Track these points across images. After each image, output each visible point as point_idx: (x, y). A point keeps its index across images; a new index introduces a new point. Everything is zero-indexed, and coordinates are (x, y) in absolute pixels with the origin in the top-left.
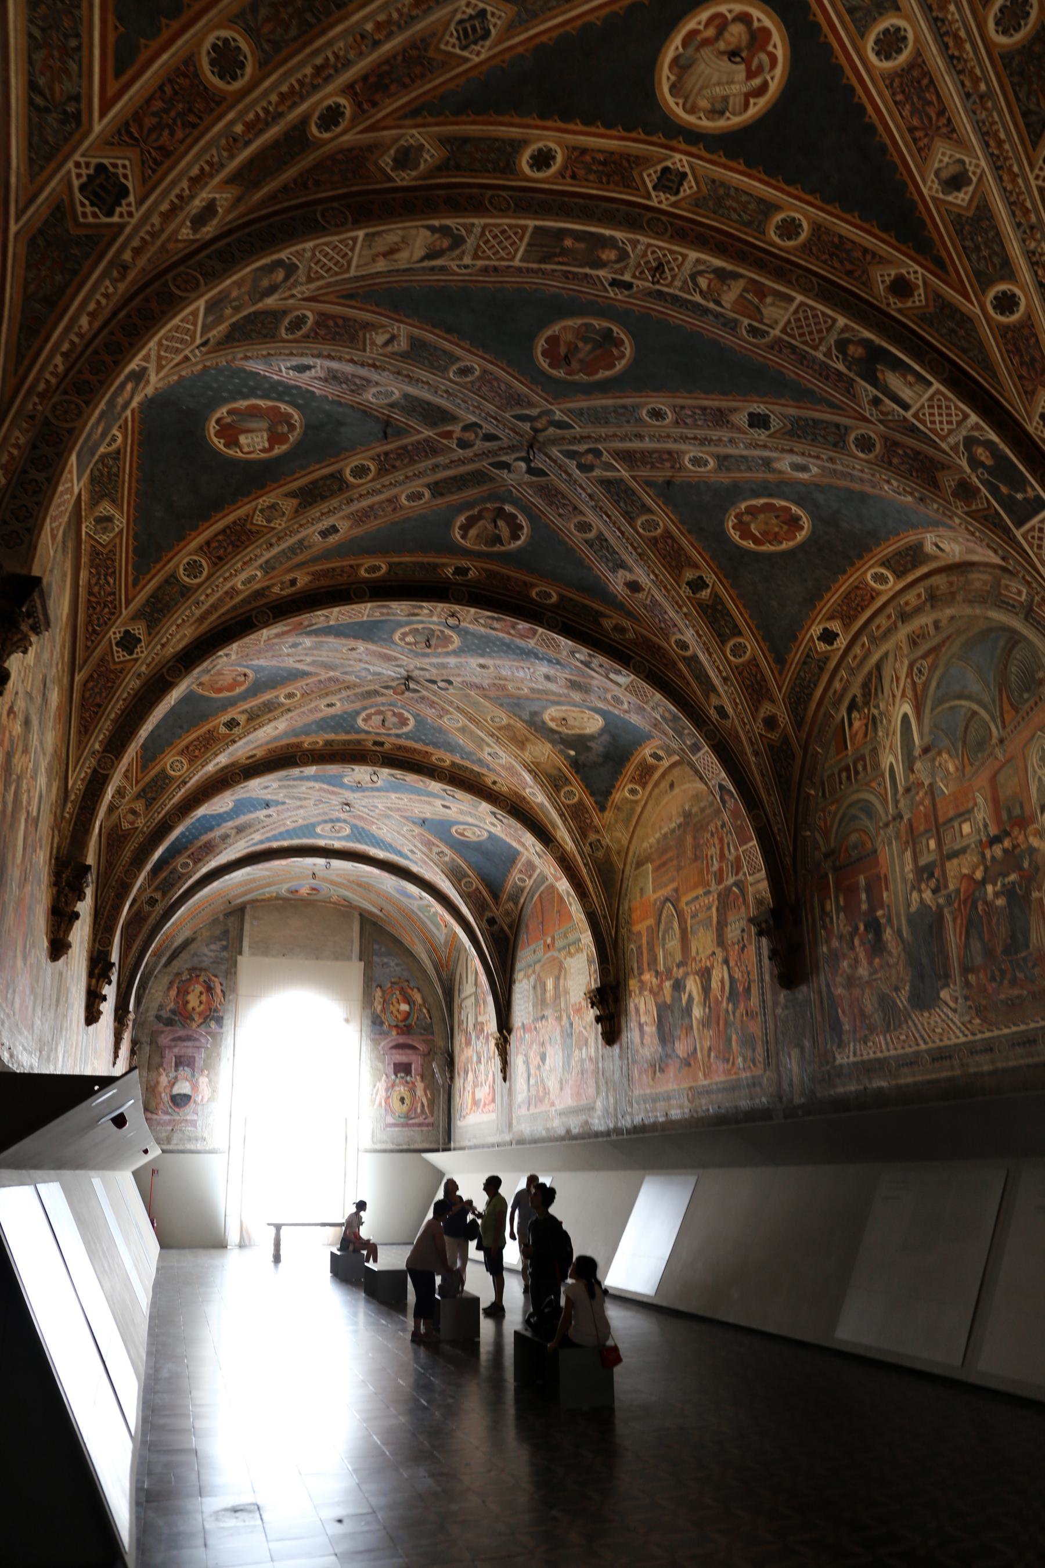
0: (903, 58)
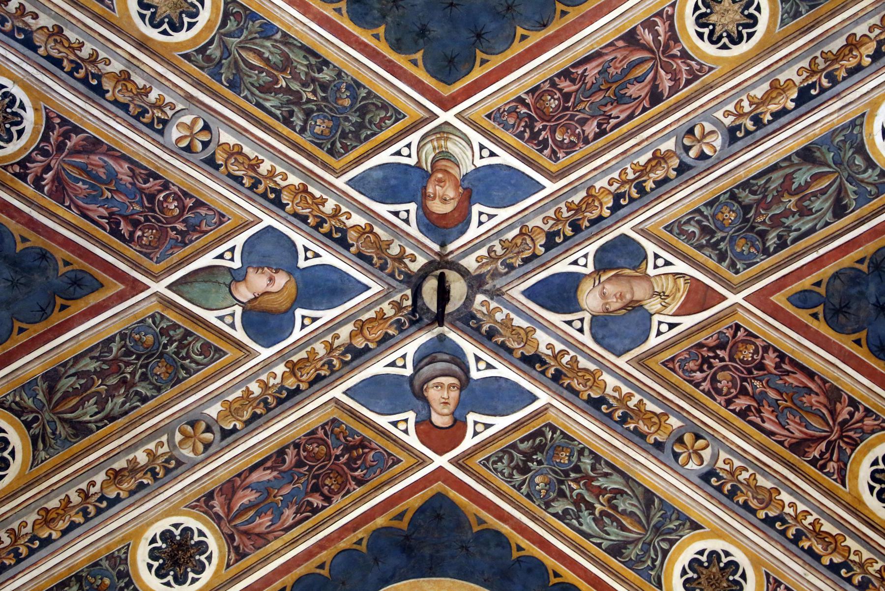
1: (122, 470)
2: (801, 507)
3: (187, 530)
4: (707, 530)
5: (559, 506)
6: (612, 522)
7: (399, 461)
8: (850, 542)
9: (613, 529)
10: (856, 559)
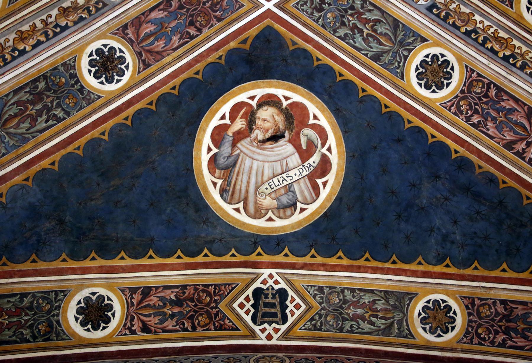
0: (456, 80)
1: (68, 8)
2: (487, 23)
3: (112, 49)
4: (431, 41)
5: (342, 32)
6: (374, 40)
7: (243, 6)
8: (515, 42)
9: (374, 44)
10: (519, 51)
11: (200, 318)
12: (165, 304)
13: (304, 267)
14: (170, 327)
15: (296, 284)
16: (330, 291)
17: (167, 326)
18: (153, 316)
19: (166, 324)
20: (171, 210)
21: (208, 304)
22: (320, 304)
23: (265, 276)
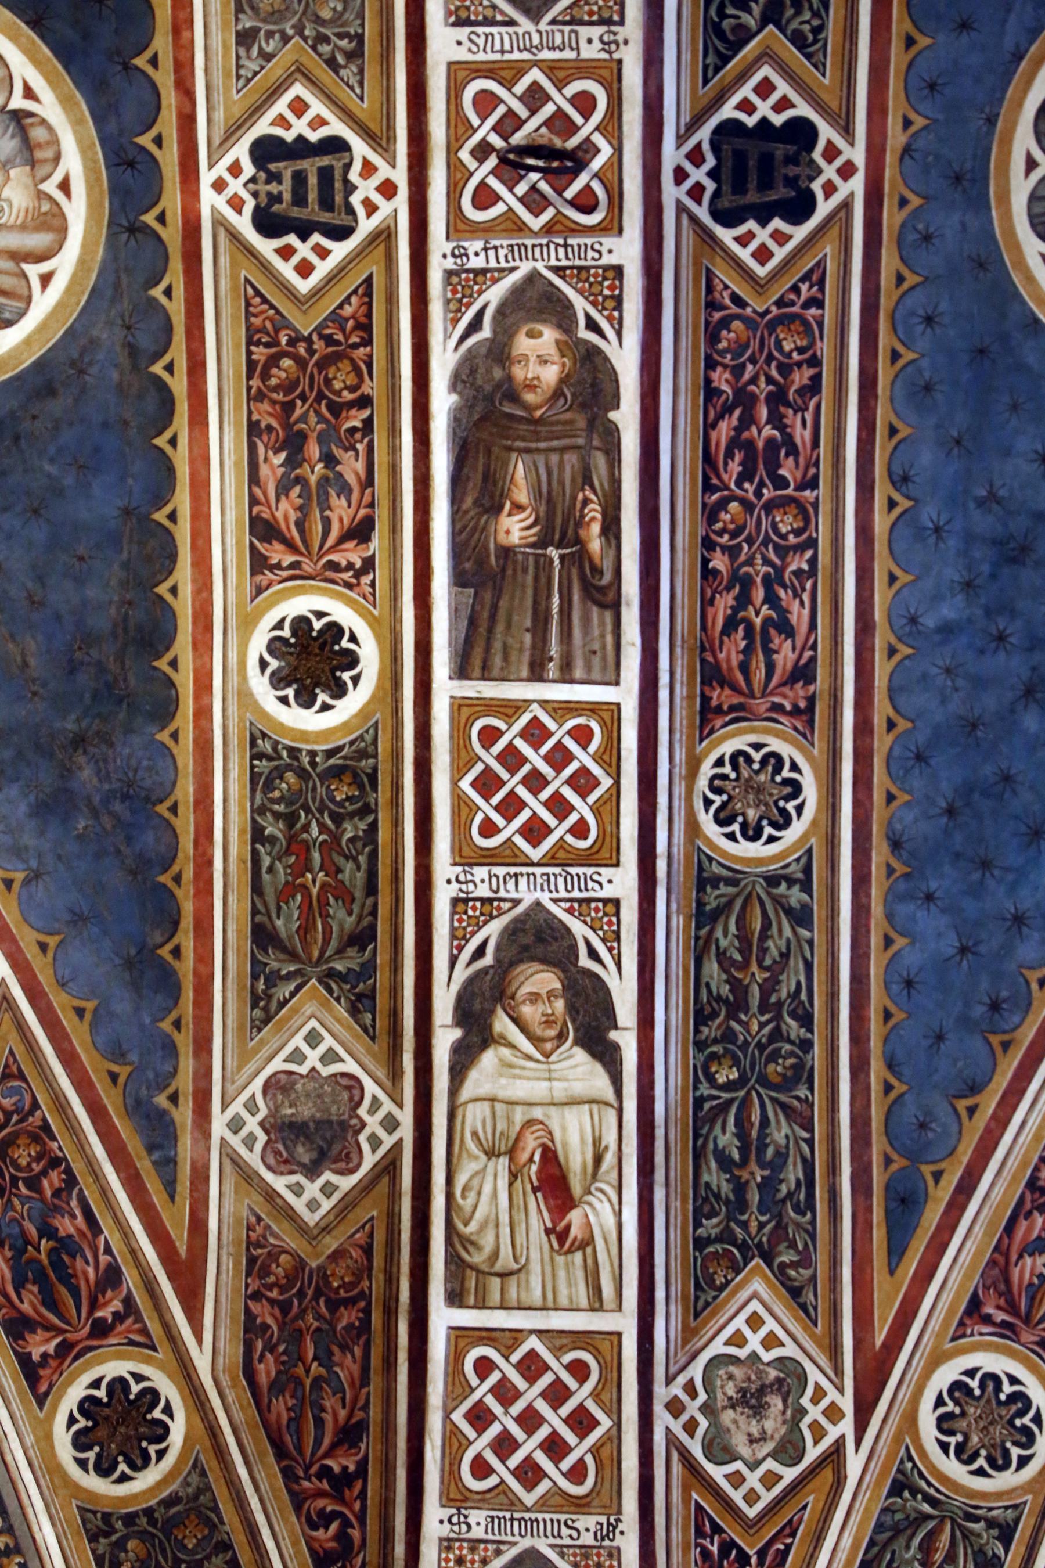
11: (337, 385)
12: (298, 480)
13: (186, 90)
14: (360, 466)
15: (237, 112)
16: (247, 8)
17: (357, 474)
18: (327, 513)
19: (351, 479)
20: (52, 461)
21: (301, 363)
22: (286, 39)
23: (220, 202)
